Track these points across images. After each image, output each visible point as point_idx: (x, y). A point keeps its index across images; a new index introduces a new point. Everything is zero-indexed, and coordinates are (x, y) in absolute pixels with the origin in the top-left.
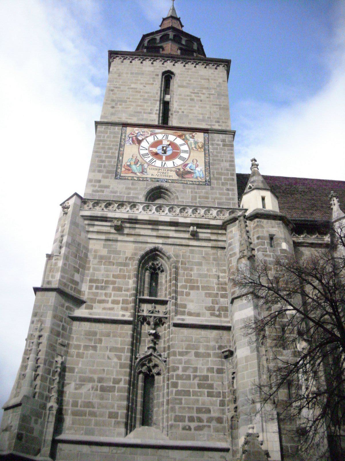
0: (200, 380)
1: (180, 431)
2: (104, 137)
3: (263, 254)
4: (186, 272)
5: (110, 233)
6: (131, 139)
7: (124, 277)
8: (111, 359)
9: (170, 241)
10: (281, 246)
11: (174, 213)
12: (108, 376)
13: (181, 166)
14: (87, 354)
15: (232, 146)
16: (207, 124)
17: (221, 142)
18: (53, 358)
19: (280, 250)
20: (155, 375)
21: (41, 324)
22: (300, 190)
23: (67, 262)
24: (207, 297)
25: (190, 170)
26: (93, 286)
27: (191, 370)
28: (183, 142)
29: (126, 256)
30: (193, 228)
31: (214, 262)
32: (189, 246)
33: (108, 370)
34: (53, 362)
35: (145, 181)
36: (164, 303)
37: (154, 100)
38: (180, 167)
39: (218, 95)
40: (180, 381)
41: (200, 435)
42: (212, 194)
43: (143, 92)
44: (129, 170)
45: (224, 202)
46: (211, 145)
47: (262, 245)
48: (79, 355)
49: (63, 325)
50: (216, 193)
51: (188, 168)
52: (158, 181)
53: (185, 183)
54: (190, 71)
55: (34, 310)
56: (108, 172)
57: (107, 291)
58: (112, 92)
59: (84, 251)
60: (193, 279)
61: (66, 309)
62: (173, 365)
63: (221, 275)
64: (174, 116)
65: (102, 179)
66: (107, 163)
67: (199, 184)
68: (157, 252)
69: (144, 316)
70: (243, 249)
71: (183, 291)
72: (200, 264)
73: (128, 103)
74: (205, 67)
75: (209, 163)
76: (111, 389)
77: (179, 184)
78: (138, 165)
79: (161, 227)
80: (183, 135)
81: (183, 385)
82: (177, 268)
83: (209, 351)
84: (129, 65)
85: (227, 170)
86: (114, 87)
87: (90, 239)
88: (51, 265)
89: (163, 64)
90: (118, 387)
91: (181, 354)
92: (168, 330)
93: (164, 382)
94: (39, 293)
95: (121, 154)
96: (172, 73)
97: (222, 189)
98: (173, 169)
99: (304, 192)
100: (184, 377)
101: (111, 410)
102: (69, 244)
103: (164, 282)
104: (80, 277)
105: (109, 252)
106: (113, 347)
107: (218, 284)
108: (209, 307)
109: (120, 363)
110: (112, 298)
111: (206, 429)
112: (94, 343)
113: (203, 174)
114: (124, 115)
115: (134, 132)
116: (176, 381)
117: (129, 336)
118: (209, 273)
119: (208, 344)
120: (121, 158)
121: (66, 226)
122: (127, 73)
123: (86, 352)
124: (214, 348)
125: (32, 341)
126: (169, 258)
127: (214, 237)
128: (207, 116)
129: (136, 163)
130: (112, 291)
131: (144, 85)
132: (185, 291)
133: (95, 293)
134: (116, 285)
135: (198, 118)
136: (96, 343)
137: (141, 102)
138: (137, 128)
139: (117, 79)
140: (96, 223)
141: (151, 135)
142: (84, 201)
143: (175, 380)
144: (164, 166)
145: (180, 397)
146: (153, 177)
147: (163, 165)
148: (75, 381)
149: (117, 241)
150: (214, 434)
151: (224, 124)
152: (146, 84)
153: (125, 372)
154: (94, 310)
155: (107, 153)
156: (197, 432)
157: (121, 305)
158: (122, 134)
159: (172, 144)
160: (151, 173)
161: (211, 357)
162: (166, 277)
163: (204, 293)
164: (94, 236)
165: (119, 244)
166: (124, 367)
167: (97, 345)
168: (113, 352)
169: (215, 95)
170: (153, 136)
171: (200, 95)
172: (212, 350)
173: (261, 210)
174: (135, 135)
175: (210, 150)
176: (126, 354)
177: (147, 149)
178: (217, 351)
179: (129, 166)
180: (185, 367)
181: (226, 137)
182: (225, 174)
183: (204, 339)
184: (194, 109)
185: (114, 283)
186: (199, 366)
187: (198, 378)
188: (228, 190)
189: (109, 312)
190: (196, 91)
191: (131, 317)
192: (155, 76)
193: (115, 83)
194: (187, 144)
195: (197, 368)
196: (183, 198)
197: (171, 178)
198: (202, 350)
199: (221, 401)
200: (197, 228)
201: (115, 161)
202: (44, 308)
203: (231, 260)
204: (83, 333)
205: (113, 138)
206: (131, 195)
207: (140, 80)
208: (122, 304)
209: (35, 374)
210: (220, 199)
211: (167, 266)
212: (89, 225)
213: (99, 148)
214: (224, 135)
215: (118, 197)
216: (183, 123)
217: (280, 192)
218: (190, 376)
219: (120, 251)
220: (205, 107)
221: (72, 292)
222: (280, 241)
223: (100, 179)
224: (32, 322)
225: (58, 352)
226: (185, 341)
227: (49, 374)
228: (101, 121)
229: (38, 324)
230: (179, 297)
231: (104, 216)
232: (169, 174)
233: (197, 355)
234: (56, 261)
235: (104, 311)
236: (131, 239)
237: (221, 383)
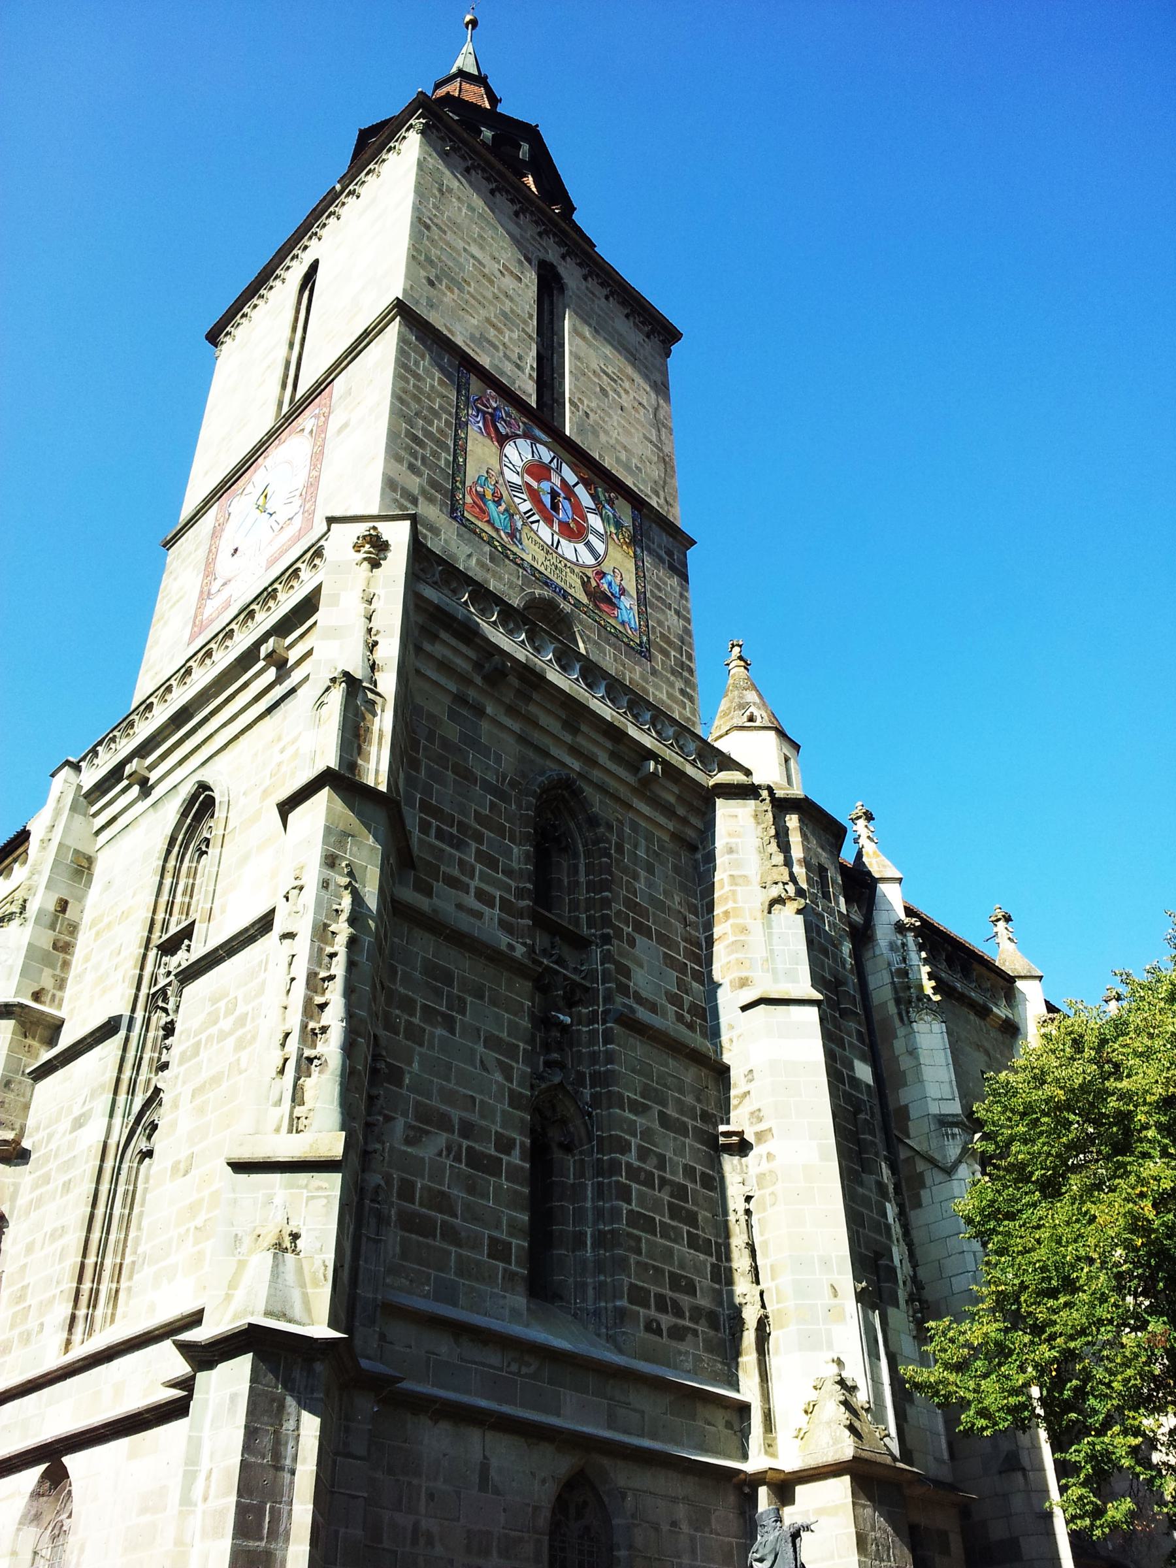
1: (642, 1334)
5: (469, 682)
7: (500, 830)
9: (596, 775)
12: (484, 1123)
14: (432, 1034)
16: (634, 484)
26: (430, 824)
27: (654, 1160)
32: (630, 807)
33: (482, 1101)
40: (634, 1186)
41: (680, 1353)
48: (416, 1036)
52: (546, 584)
54: (597, 301)
56: (433, 484)
65: (421, 499)
67: (628, 645)
72: (650, 869)
76: (492, 1167)
78: (502, 508)
79: (584, 728)
81: (642, 1198)
83: (686, 1119)
86: (430, 219)
90: (508, 1164)
93: (582, 1175)
95: (460, 449)
96: (558, 278)
98: (577, 570)
101: (495, 1234)
107: (685, 940)
111: (690, 1337)
115: (488, 400)
120: (461, 460)
123: (428, 1028)
126: (593, 821)
127: (681, 811)
129: (498, 503)
140: (444, 635)
141: (526, 436)
145: (635, 1232)
146: (535, 565)
148: (405, 1114)
149: (480, 712)
150: (705, 1356)
153: (522, 1120)
156: (674, 1344)
160: (531, 553)
174: (490, 410)
178: (699, 1124)
186: (669, 1154)
187: (667, 1188)
190: (609, 371)
198: (671, 1112)
199: (713, 1265)
203: (734, 892)
226: (639, 1073)
233: (664, 1120)
236: (516, 726)
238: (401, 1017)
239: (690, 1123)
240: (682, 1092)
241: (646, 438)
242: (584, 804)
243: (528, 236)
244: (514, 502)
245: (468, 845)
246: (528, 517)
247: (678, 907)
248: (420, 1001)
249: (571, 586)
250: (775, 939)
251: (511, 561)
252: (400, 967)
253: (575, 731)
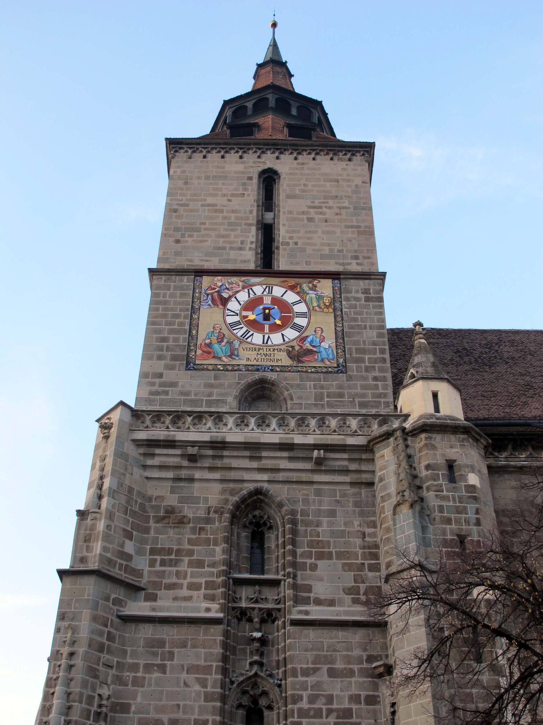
0: (338, 718)
2: (165, 296)
3: (436, 496)
4: (309, 529)
6: (210, 297)
7: (207, 542)
8: (190, 687)
9: (281, 476)
10: (466, 480)
11: (286, 428)
12: (186, 717)
13: (295, 341)
14: (150, 679)
15: (381, 300)
16: (336, 263)
17: (363, 293)
18: (94, 690)
19: (465, 486)
20: (264, 709)
21: (73, 633)
22: (506, 355)
23: (111, 523)
24: (345, 571)
26: (156, 560)
27: (323, 700)
28: (297, 298)
29: (210, 503)
30: (319, 454)
31: (357, 509)
32: (312, 483)
33: (185, 705)
34: (94, 697)
35: (236, 370)
36: (276, 583)
37: (246, 224)
38: (294, 343)
39: (355, 208)
42: (350, 387)
43: (228, 212)
44: (209, 353)
46: (345, 300)
47: (434, 480)
48: (137, 682)
49: (109, 632)
50: (355, 387)
51: (307, 345)
52: (258, 370)
53: (302, 372)
55: (59, 608)
56: (174, 358)
57: (177, 569)
58: (175, 214)
59: (139, 501)
60: (322, 541)
61: (113, 604)
62: (293, 692)
63: (368, 530)
64: (281, 251)
66: (171, 343)
67: (326, 372)
68: (260, 496)
69: (242, 607)
70: (401, 488)
71: (306, 563)
72: (332, 513)
73: (203, 232)
74: (332, 159)
75: (343, 334)
77: (293, 373)
78: (223, 344)
79: (264, 454)
80: (298, 284)
82: (294, 522)
83: (351, 666)
84: (201, 162)
85: (374, 344)
87: (147, 478)
88: (86, 530)
89: (259, 157)
91: (306, 673)
92: (283, 630)
94: (68, 580)
95: (194, 325)
96: (275, 173)
98: (283, 347)
99: (513, 358)
100: (312, 713)
102: (114, 491)
103: (273, 546)
104: (134, 545)
105: (182, 500)
106: (193, 665)
107: (364, 548)
108: (349, 589)
109: (205, 692)
110: (189, 580)
112: (161, 660)
113: (333, 354)
114: (196, 254)
116: (299, 720)
117: (218, 644)
118: (347, 529)
119: (350, 653)
120: (194, 332)
121: (107, 460)
122: (199, 178)
123: (147, 676)
124: (360, 661)
125: (59, 663)
126: (280, 505)
127: (353, 466)
128: (336, 248)
130: (188, 567)
131: (229, 198)
132: (309, 561)
133: (159, 572)
134: (195, 557)
135: (323, 252)
136: (164, 660)
137: (225, 230)
138: (219, 278)
139: (181, 189)
140: (158, 451)
141: (243, 288)
142: (136, 414)
143: (296, 719)
144: (267, 343)
146: (249, 363)
147: (265, 342)
151: (366, 261)
152: (233, 195)
153: (214, 707)
154: (159, 603)
155: (170, 324)
157: (203, 591)
158: (194, 289)
159: (277, 301)
161: (355, 677)
162: (277, 539)
163: (340, 565)
164: (156, 474)
165: (196, 485)
166: (212, 700)
167: (166, 662)
168: (194, 674)
169: (349, 208)
170: (246, 290)
171: (324, 210)
172: (357, 665)
173: (431, 416)
174: (217, 290)
175: (344, 310)
176: (214, 676)
177: (237, 314)
179: (209, 345)
180: (312, 694)
181: (369, 285)
182: (370, 352)
183: (343, 644)
184: (315, 236)
185: (191, 553)
186: (335, 693)
187: (334, 714)
188: (375, 379)
189: (184, 604)
190: (316, 204)
191: (221, 612)
192: (246, 181)
193: (179, 197)
194: (305, 301)
195: (332, 696)
196: (300, 398)
197: (279, 364)
198: (339, 665)
200: (326, 451)
201: (186, 338)
202: (77, 605)
203: (383, 507)
204: (142, 643)
205: (179, 298)
206: (214, 398)
207: (221, 189)
208: (205, 589)
209: (65, 721)
210: (363, 396)
211: (278, 520)
212: (145, 455)
213: (156, 317)
214: (367, 281)
215: (194, 402)
216: (297, 264)
217: (471, 363)
218: (321, 710)
219: (200, 497)
220: (334, 233)
221: (123, 573)
222: (465, 472)
223: (161, 370)
224: (58, 630)
225: (102, 677)
226: (312, 650)
227: (89, 719)
228: (158, 267)
229: (67, 634)
230: (299, 573)
231: (170, 439)
232: (276, 357)
234: (93, 522)
235: (177, 604)
236: (217, 475)
237: (373, 721)
238: (129, 675)
239: (356, 667)
240: (348, 649)
241: (347, 227)
242: (271, 497)
243: (251, 164)
244: (233, 334)
245: (183, 560)
246: (244, 338)
247: (357, 528)
248: (142, 662)
249: (278, 360)
250: (398, 531)
251: (231, 370)
252: (129, 649)
253: (260, 458)
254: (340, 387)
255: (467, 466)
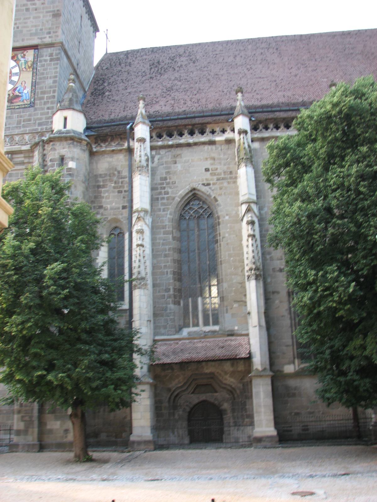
10: (67, 165)
16: (38, 38)
17: (49, 56)
25: (18, 94)
42: (35, 115)
45: (43, 122)
51: (17, 93)
53: (12, 109)
85: (51, 87)
97: (43, 109)
135: (32, 32)
175: (38, 68)
188: (48, 108)
210: (41, 119)
214: (52, 48)
254: (30, 115)
255: (69, 158)
